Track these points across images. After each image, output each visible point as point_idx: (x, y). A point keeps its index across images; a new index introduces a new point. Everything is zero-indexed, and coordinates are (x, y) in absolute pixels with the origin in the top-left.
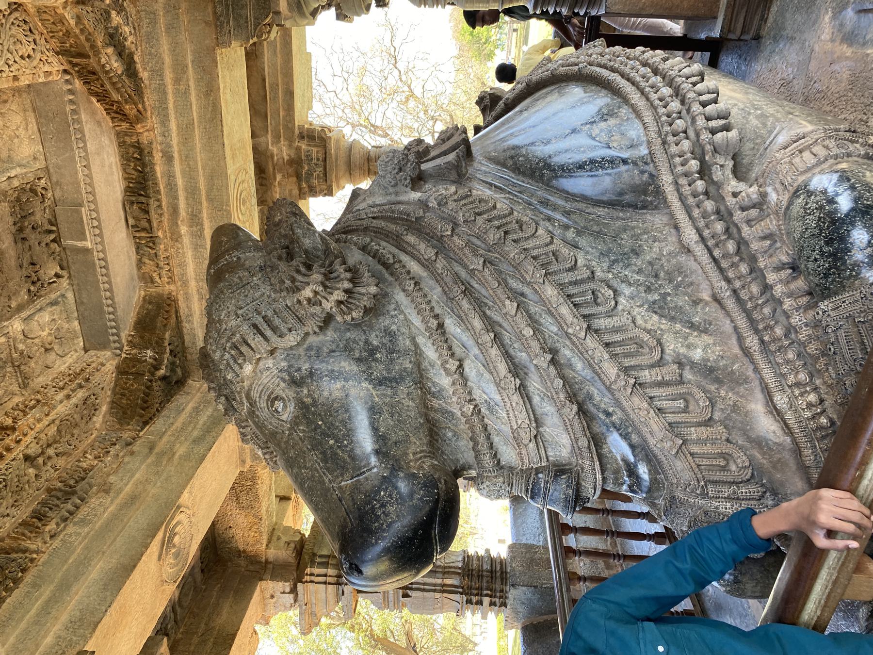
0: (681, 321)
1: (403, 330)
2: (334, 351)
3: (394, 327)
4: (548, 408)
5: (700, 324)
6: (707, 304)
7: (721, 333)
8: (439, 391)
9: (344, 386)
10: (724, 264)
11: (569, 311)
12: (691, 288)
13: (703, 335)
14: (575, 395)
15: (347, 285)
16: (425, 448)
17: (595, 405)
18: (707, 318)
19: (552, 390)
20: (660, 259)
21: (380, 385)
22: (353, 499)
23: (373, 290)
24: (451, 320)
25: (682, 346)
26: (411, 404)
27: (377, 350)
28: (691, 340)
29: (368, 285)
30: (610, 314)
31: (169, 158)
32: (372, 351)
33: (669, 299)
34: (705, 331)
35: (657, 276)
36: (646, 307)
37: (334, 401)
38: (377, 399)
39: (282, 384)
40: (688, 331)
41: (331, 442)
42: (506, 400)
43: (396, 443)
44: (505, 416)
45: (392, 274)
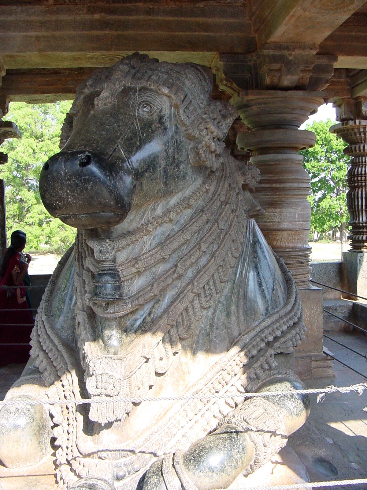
3: (187, 178)
31: (149, 12)
39: (158, 111)
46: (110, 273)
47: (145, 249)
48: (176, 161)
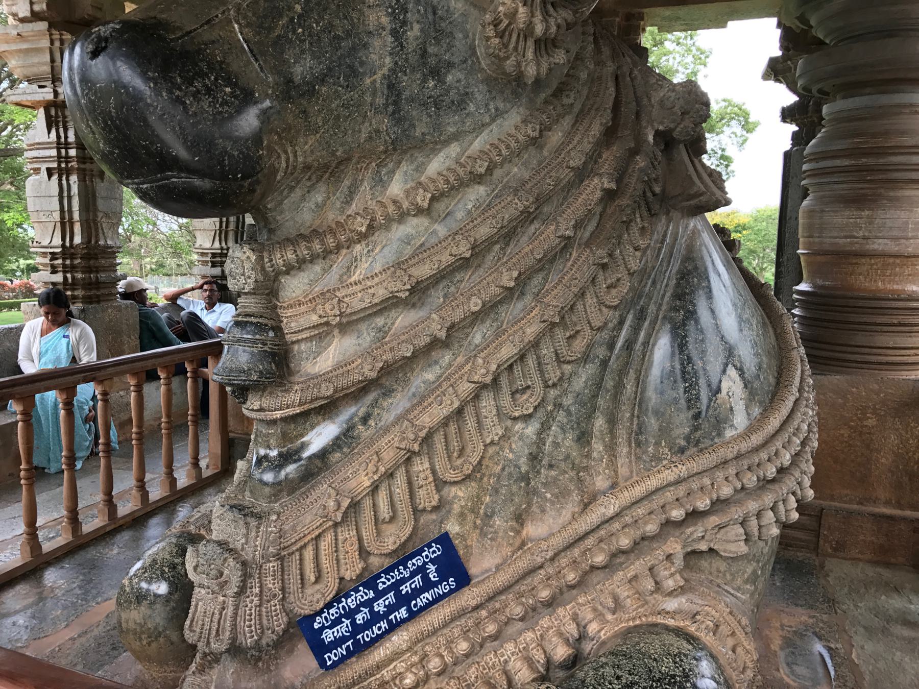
0: (493, 502)
1: (469, 122)
2: (435, 13)
3: (472, 107)
4: (368, 339)
5: (492, 526)
6: (518, 532)
7: (481, 554)
8: (381, 180)
9: (384, 29)
10: (576, 552)
11: (505, 358)
12: (538, 511)
13: (478, 531)
14: (389, 373)
15: (539, 29)
16: (300, 159)
17: (376, 401)
18: (500, 534)
19: (395, 343)
20: (572, 469)
21: (388, 87)
22: (213, 42)
23: (531, 71)
24: (484, 194)
25: (462, 507)
26: (364, 135)
27: (439, 81)
28: (470, 517)
29: (538, 64)
30: (500, 414)
32: (436, 73)
33: (523, 484)
34: (483, 534)
35: (551, 466)
36: (511, 456)
37: (361, 12)
38: (368, 81)
40: (482, 512)
41: (298, 8)
42: (376, 280)
43: (305, 112)
44: (352, 279)
45: (546, 102)
46: (247, 322)
47: (358, 272)
48: (432, 61)
